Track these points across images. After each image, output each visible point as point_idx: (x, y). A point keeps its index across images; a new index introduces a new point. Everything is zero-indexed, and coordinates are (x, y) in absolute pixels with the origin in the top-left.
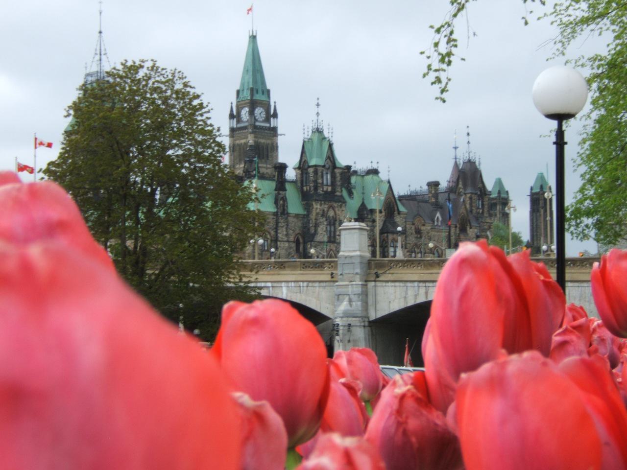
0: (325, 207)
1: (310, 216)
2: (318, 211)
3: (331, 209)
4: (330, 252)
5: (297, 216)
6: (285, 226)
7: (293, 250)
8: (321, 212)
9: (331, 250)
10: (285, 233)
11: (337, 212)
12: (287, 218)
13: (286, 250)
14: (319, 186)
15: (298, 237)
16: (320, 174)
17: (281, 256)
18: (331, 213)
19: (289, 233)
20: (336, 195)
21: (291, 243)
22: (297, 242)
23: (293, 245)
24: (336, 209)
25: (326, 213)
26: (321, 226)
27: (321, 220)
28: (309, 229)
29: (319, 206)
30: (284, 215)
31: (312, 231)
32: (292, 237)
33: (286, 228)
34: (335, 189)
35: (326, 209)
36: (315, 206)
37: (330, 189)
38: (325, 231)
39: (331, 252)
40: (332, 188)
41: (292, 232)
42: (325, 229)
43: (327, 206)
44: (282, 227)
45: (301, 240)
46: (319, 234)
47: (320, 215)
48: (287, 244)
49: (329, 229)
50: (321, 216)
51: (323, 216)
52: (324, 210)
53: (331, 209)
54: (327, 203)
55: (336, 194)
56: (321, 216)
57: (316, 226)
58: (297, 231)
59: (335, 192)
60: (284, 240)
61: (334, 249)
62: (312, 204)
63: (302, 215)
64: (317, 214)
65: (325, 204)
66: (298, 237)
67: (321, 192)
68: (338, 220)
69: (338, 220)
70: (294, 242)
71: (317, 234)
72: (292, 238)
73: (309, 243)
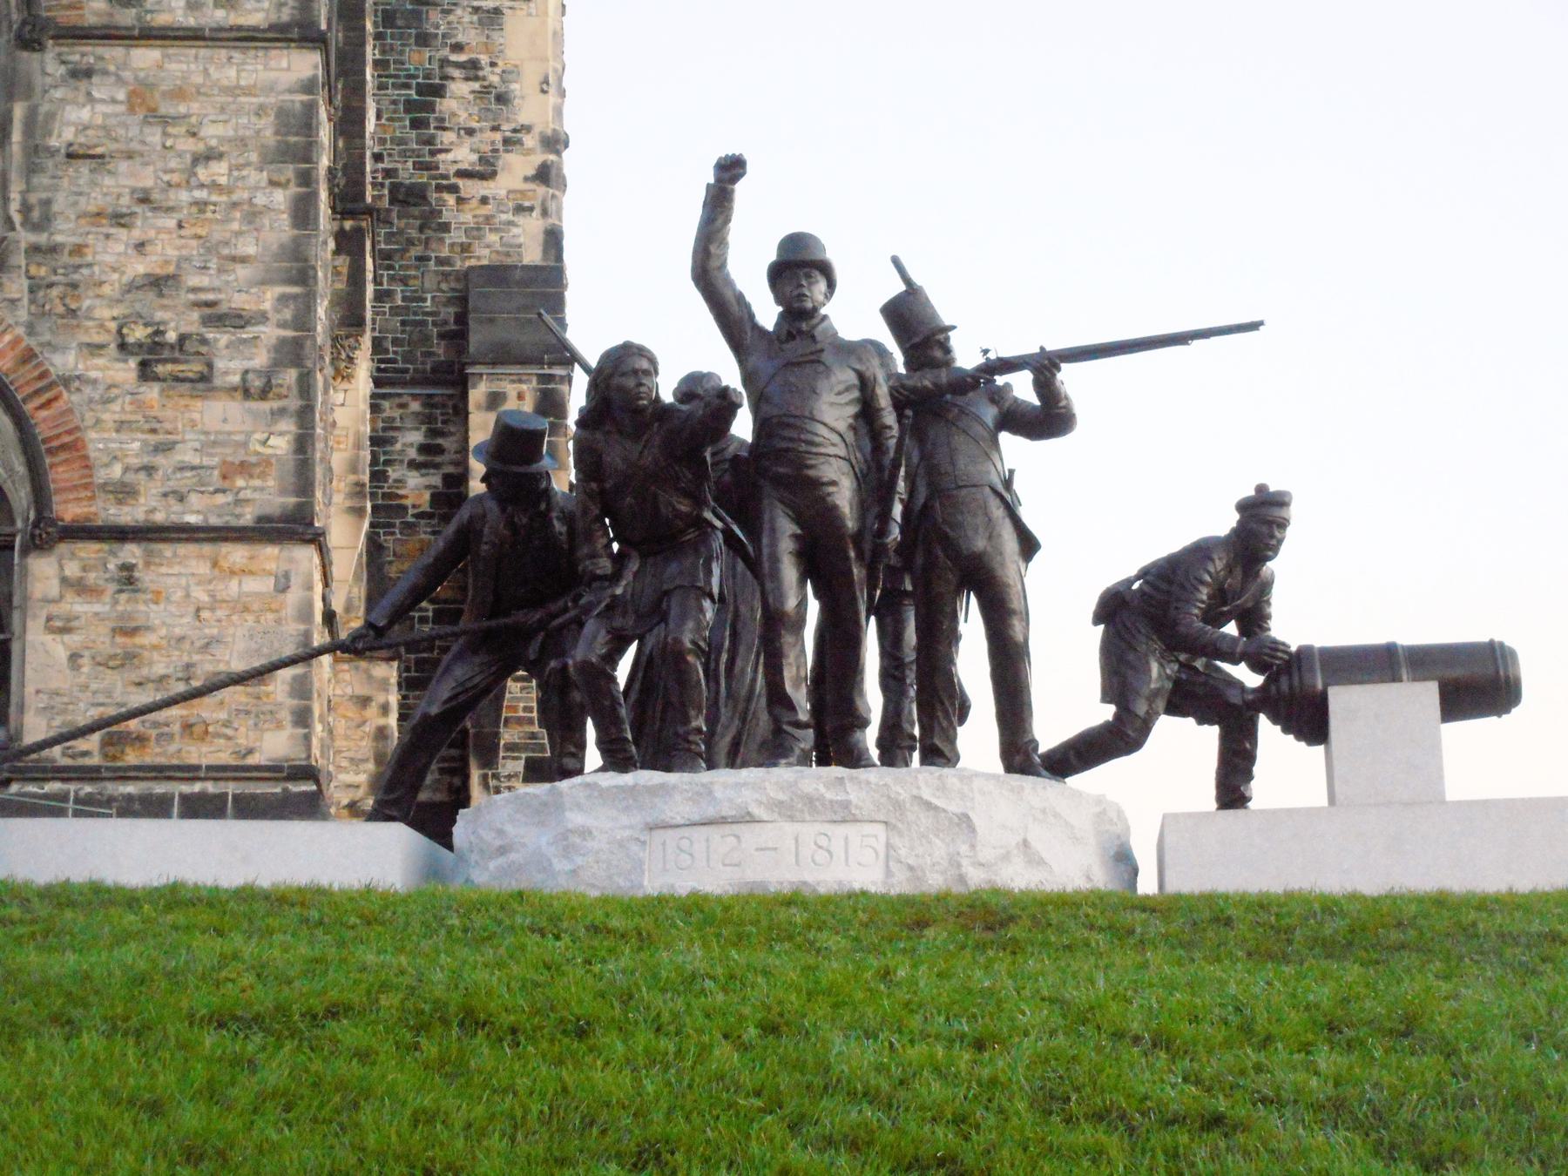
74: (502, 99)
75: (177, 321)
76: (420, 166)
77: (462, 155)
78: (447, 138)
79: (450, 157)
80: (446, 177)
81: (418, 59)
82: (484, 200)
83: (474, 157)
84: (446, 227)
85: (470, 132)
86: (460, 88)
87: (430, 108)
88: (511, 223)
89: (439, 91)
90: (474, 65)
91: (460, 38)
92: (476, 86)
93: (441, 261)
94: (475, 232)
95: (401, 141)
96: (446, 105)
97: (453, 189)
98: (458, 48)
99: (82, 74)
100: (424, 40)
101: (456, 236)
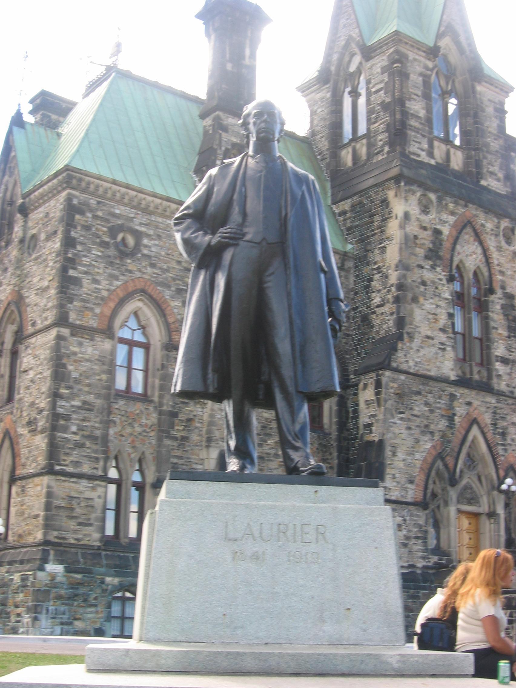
0: (446, 222)
1: (376, 256)
2: (413, 228)
3: (468, 236)
4: (468, 431)
8: (426, 237)
9: (475, 421)
11: (495, 257)
14: (417, 130)
16: (415, 79)
18: (469, 255)
20: (486, 189)
24: (491, 243)
25: (447, 245)
26: (429, 305)
27: (428, 275)
28: (366, 320)
29: (415, 210)
31: (384, 322)
34: (478, 164)
35: (446, 230)
36: (398, 207)
37: (457, 161)
38: (443, 330)
39: (475, 431)
40: (468, 158)
42: (443, 320)
43: (452, 219)
46: (417, 342)
47: (421, 252)
49: (459, 328)
50: (427, 257)
51: (434, 254)
52: (437, 232)
53: (468, 236)
54: (451, 206)
55: (483, 183)
56: (427, 257)
57: (404, 294)
59: (479, 176)
61: (487, 419)
62: (385, 202)
64: (409, 242)
65: (441, 206)
67: (424, 157)
68: (499, 293)
69: (499, 293)
71: (411, 337)
73: (370, 379)
74: (387, 277)
75: (34, 414)
76: (368, 307)
77: (377, 300)
78: (374, 295)
79: (373, 302)
80: (373, 309)
81: (366, 270)
82: (382, 314)
83: (380, 299)
84: (373, 327)
85: (379, 291)
86: (377, 277)
87: (368, 286)
88: (389, 320)
89: (371, 280)
90: (379, 268)
91: (376, 260)
92: (380, 275)
93: (373, 338)
94: (380, 326)
95: (363, 300)
96: (373, 283)
97: (374, 313)
98: (375, 263)
99: (27, 347)
100: (368, 264)
101: (376, 329)
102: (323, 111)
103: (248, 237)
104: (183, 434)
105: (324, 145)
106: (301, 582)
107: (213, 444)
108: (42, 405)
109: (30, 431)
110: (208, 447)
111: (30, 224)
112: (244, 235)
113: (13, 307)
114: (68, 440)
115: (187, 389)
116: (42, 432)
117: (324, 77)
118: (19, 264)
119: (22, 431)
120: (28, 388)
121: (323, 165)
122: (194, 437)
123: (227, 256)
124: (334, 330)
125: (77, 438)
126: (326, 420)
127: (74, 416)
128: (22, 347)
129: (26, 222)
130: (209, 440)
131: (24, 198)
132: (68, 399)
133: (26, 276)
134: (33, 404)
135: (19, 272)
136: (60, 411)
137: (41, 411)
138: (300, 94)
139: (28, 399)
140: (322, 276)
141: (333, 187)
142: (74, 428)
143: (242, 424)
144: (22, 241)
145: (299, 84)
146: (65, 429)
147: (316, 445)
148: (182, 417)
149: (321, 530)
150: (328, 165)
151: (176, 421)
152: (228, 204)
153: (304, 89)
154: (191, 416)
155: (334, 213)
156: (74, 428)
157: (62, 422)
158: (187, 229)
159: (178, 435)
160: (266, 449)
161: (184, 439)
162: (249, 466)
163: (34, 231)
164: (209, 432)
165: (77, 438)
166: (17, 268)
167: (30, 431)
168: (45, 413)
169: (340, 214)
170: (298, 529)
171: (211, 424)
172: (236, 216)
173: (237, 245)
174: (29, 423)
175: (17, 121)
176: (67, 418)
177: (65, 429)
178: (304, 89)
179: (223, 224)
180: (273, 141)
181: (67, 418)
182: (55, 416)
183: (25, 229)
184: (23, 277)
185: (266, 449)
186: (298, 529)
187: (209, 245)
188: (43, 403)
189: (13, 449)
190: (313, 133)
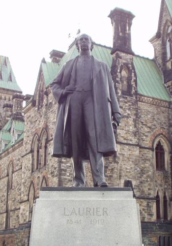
5: (156, 103)
6: (133, 117)
7: (152, 165)
10: (132, 128)
12: (136, 102)
13: (136, 163)
15: (159, 142)
17: (123, 174)
19: (142, 131)
21: (146, 151)
22: (159, 150)
23: (151, 155)
30: (131, 95)
32: (149, 139)
33: (135, 121)
41: (147, 130)
44: (128, 117)
45: (166, 147)
48: (136, 151)
58: (158, 130)
60: (131, 142)
63: (166, 101)
66: (159, 145)
70: (152, 150)
72: (147, 143)
75: (53, 170)
102: (159, 48)
103: (77, 90)
104: (110, 174)
105: (160, 61)
106: (96, 233)
107: (122, 178)
108: (56, 166)
109: (52, 176)
110: (120, 179)
111: (49, 98)
112: (75, 89)
113: (45, 130)
114: (66, 179)
115: (57, 153)
116: (56, 176)
117: (158, 36)
118: (46, 114)
119: (50, 176)
120: (51, 160)
121: (160, 69)
122: (115, 176)
123: (69, 98)
124: (114, 125)
125: (69, 178)
126: (166, 166)
127: (68, 169)
128: (48, 145)
129: (47, 98)
130: (120, 176)
131: (46, 89)
132: (65, 163)
133: (49, 118)
134: (53, 166)
135: (46, 117)
136: (62, 168)
137: (55, 168)
138: (150, 43)
139: (51, 164)
140: (109, 104)
141: (164, 77)
142: (68, 174)
143: (79, 168)
144: (46, 105)
145: (150, 39)
146: (65, 175)
147: (163, 176)
148: (110, 168)
149: (105, 210)
150: (162, 69)
151: (107, 170)
152: (70, 76)
153: (151, 41)
154: (113, 167)
155: (165, 87)
156: (68, 174)
157: (63, 172)
158: (55, 88)
159: (108, 175)
160: (143, 179)
161: (111, 176)
162: (81, 185)
163: (51, 101)
164: (120, 173)
165: (69, 178)
166: (45, 115)
167: (52, 176)
168: (57, 169)
169: (167, 87)
170: (95, 210)
171: (121, 170)
172: (72, 82)
173: (72, 93)
174: (52, 173)
175: (44, 61)
176: (65, 171)
177: (65, 175)
178: (151, 41)
179: (68, 85)
180: (88, 49)
181: (65, 171)
182: (60, 170)
183: (47, 100)
184: (47, 118)
185: (143, 179)
186: (95, 210)
187: (62, 94)
188: (56, 165)
189: (46, 183)
190: (156, 57)
